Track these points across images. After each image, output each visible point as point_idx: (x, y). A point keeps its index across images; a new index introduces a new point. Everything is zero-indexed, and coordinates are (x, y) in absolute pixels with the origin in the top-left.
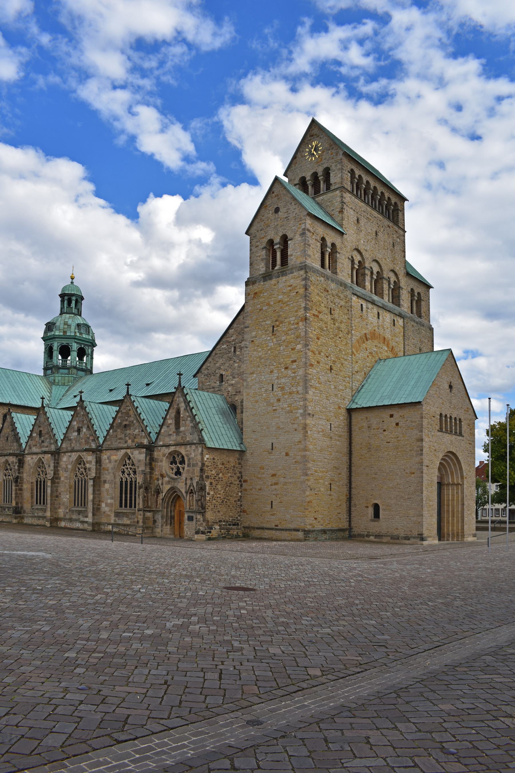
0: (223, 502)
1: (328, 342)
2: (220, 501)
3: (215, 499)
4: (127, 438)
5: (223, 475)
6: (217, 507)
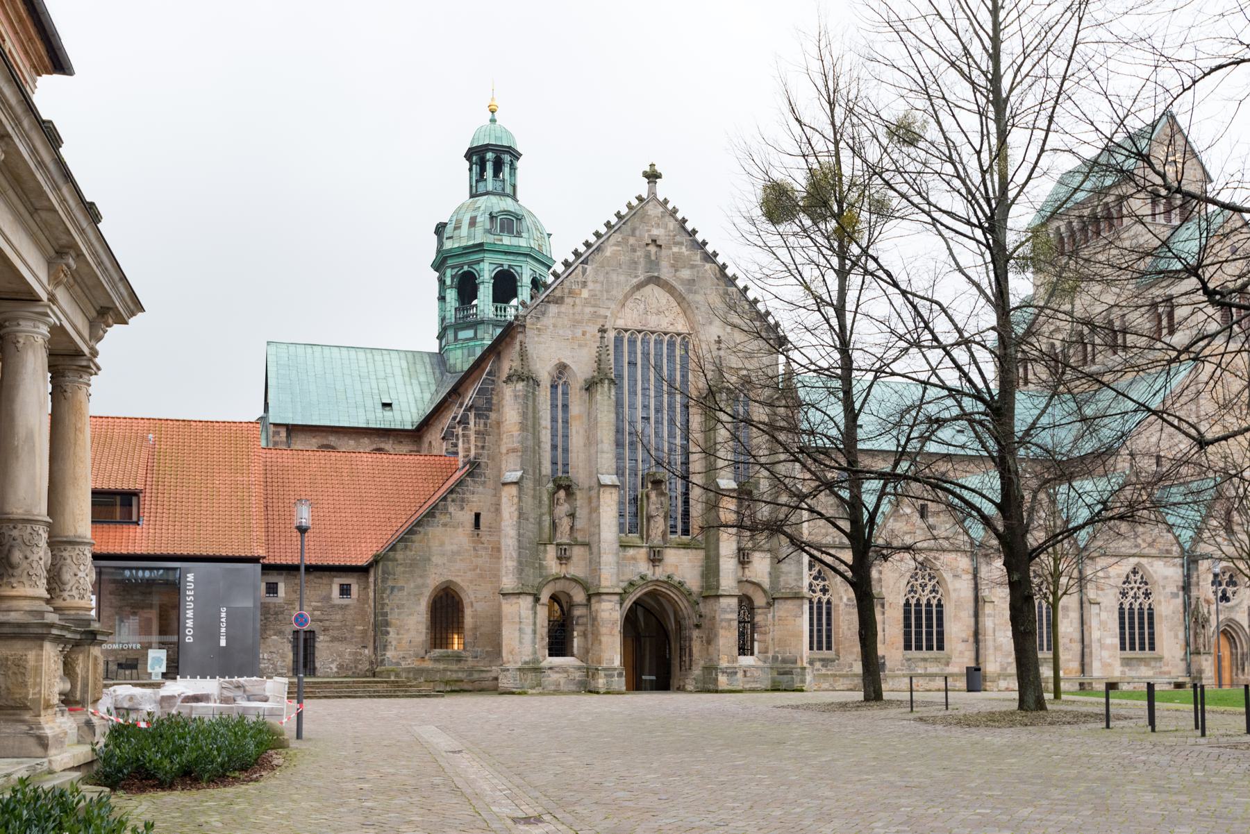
4: (1139, 541)
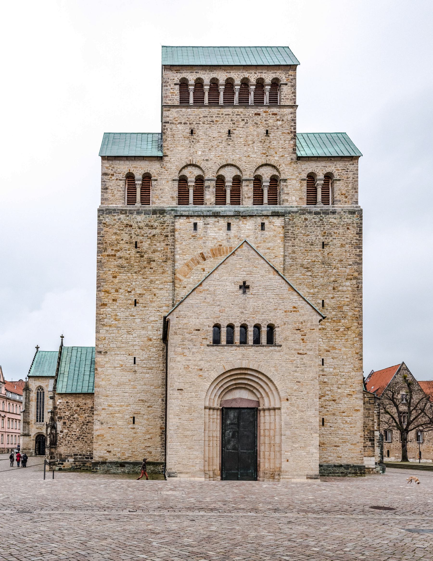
0: (78, 438)
1: (131, 277)
2: (75, 437)
3: (69, 436)
5: (79, 415)
6: (71, 442)
